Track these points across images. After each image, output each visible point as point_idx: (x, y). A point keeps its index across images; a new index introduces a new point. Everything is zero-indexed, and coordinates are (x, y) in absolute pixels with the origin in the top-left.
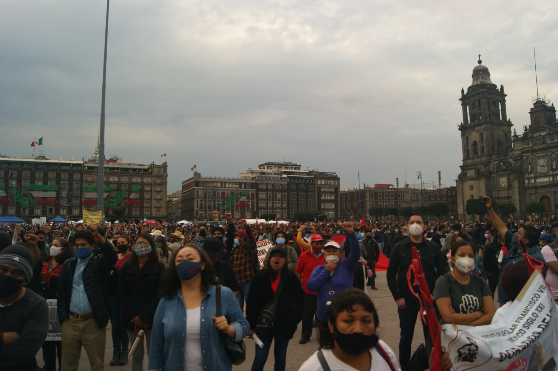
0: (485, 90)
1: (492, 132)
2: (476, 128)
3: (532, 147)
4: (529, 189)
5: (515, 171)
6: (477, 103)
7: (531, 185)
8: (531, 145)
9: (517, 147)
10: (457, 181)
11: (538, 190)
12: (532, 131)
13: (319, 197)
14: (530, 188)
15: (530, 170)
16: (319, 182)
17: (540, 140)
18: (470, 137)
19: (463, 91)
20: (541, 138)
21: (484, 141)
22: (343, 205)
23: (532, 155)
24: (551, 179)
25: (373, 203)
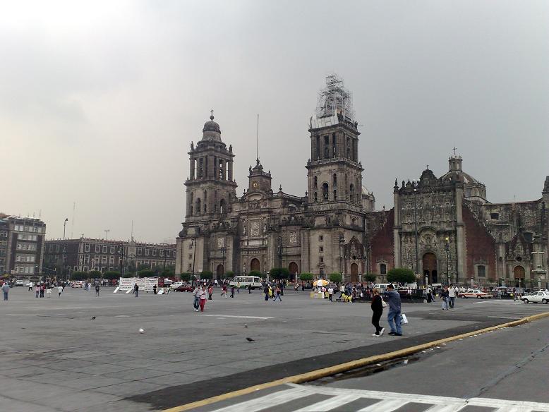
0: (213, 148)
2: (201, 186)
6: (204, 159)
9: (236, 208)
14: (243, 250)
15: (244, 232)
16: (16, 228)
19: (192, 146)
21: (208, 199)
24: (261, 242)
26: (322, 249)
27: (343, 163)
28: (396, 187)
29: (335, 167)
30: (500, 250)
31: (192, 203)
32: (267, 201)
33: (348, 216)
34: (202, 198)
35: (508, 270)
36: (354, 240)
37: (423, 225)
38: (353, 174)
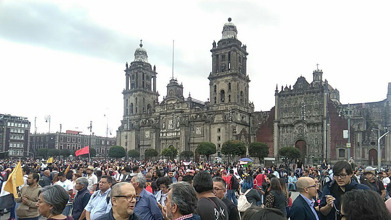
0: (142, 66)
1: (144, 98)
2: (133, 94)
3: (166, 111)
4: (162, 140)
5: (154, 127)
6: (135, 75)
7: (164, 138)
8: (165, 110)
9: (158, 109)
10: (117, 131)
11: (168, 141)
12: (167, 100)
13: (8, 138)
15: (164, 127)
17: (171, 106)
18: (128, 99)
20: (172, 105)
22: (37, 145)
23: (166, 117)
24: (176, 134)
25: (61, 145)
26: (219, 138)
27: (236, 74)
28: (277, 91)
29: (230, 78)
30: (358, 137)
31: (127, 106)
32: (180, 104)
33: (239, 114)
34: (134, 103)
35: (363, 152)
36: (243, 131)
37: (298, 119)
38: (243, 84)
